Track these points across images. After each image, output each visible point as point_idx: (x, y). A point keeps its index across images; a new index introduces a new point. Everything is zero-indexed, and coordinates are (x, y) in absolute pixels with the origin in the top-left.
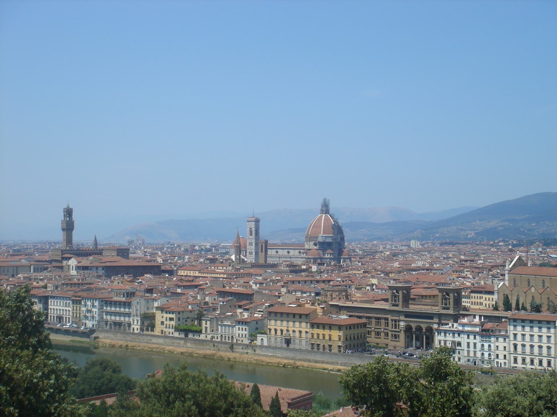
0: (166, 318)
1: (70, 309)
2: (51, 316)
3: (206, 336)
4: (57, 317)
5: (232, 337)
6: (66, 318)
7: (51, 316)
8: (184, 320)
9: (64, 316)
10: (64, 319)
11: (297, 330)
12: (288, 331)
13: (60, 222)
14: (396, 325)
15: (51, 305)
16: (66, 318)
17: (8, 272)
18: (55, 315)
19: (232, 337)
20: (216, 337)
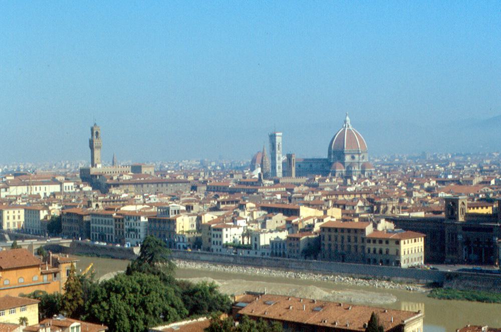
0: (214, 235)
1: (113, 227)
2: (93, 234)
3: (256, 253)
4: (99, 235)
5: (284, 253)
6: (109, 236)
7: (93, 234)
8: (232, 237)
9: (107, 234)
10: (107, 236)
11: (353, 244)
12: (343, 247)
13: (88, 141)
14: (453, 238)
15: (93, 223)
16: (109, 236)
17: (40, 190)
18: (97, 234)
19: (284, 253)
20: (266, 254)
